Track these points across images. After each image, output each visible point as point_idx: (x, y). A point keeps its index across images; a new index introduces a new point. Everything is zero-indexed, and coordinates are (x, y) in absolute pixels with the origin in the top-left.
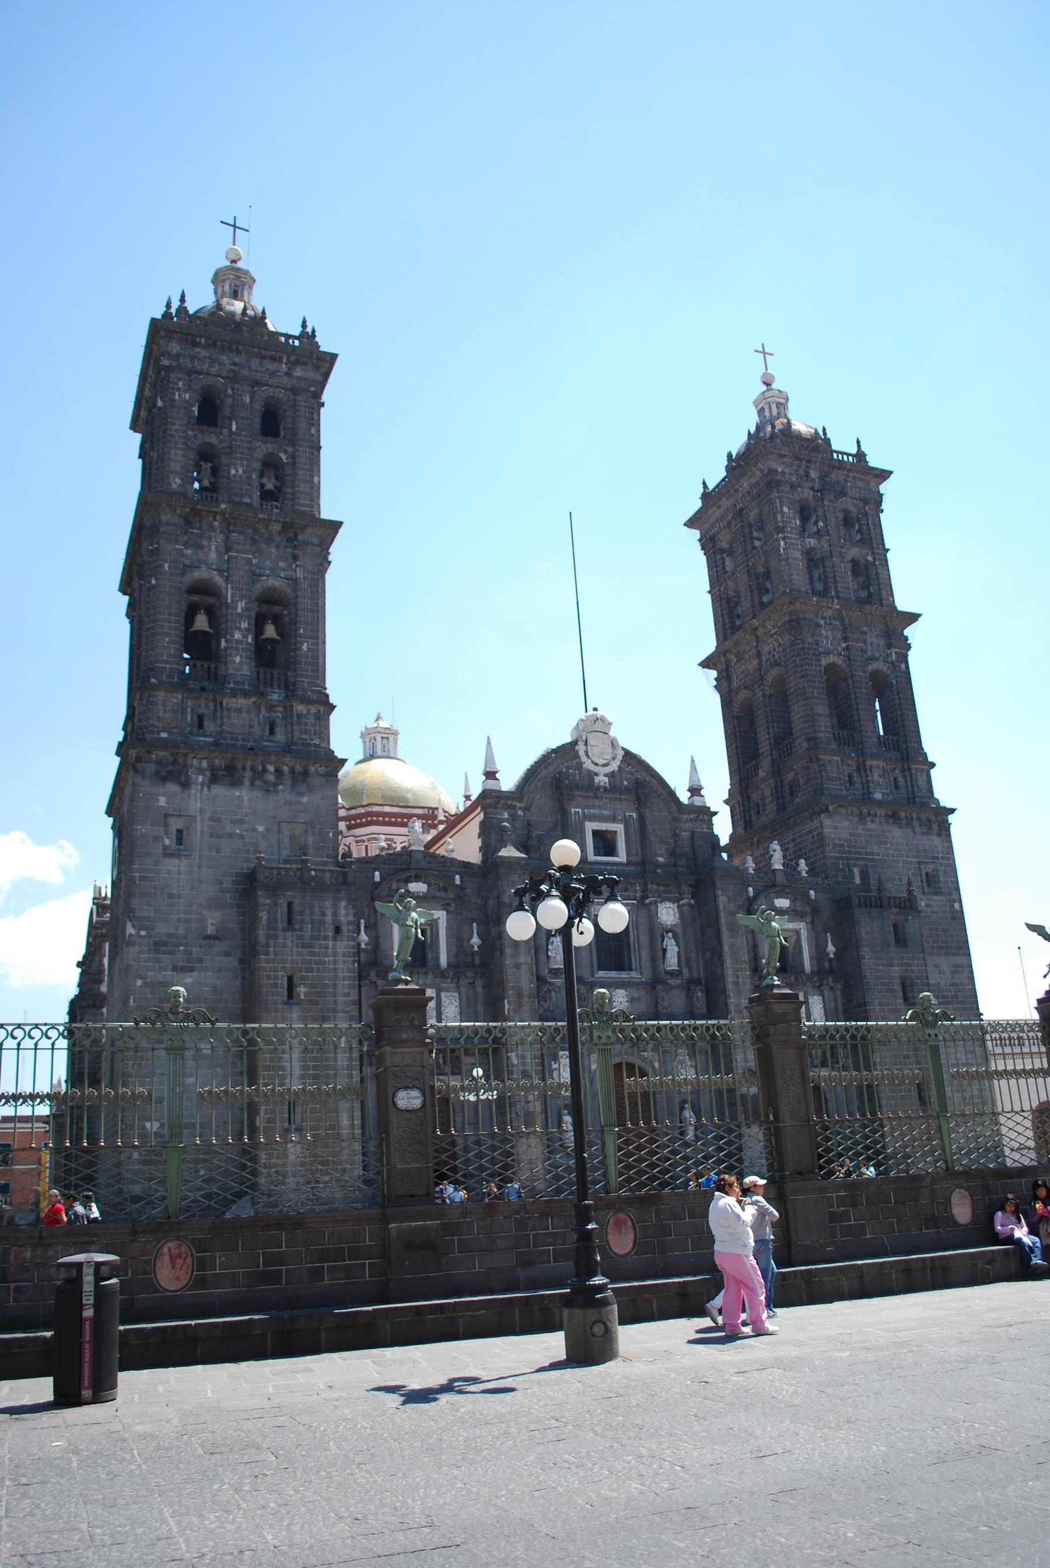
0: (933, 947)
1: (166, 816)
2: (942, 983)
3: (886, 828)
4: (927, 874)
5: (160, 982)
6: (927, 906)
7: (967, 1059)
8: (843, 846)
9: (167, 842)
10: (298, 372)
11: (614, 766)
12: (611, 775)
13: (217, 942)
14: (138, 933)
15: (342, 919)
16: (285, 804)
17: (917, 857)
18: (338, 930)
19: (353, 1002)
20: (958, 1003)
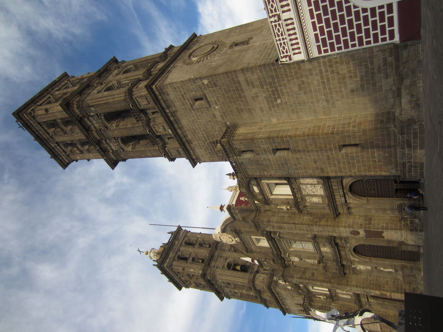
0: (242, 101)
2: (264, 95)
3: (185, 129)
4: (196, 100)
6: (217, 105)
7: (317, 74)
8: (209, 153)
10: (167, 270)
11: (230, 236)
20: (275, 83)
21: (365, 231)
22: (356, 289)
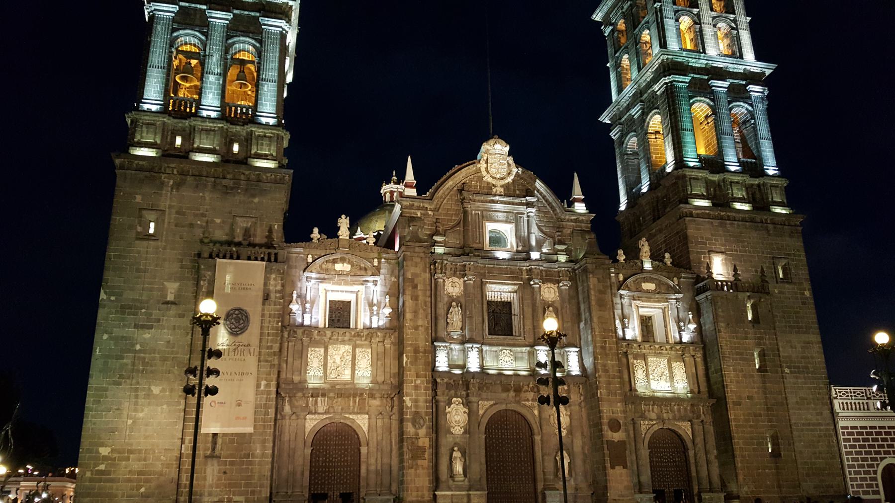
0: (785, 326)
1: (141, 209)
5: (123, 337)
6: (780, 292)
9: (139, 229)
11: (510, 179)
12: (506, 187)
13: (173, 306)
14: (109, 299)
15: (271, 288)
16: (240, 202)
17: (772, 254)
18: (266, 297)
19: (275, 354)
20: (808, 373)
21: (622, 443)
22: (422, 399)
